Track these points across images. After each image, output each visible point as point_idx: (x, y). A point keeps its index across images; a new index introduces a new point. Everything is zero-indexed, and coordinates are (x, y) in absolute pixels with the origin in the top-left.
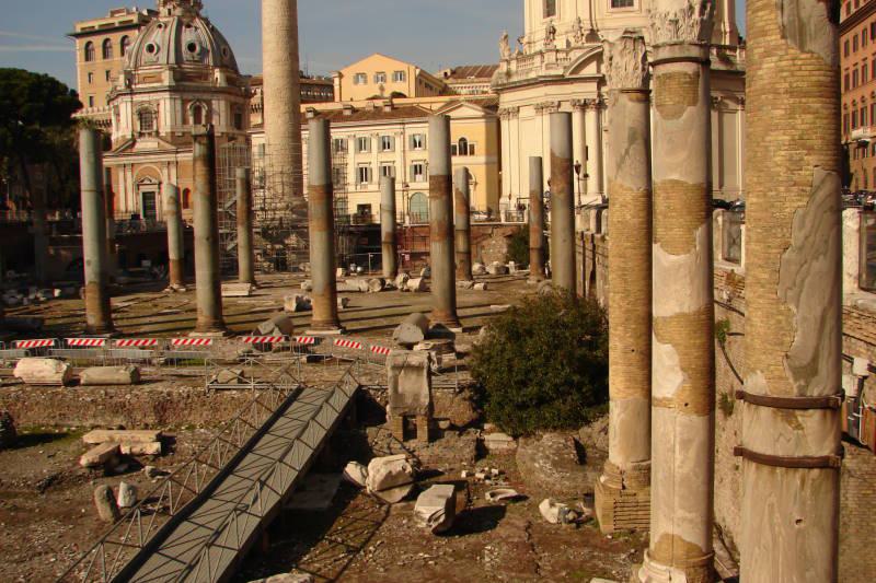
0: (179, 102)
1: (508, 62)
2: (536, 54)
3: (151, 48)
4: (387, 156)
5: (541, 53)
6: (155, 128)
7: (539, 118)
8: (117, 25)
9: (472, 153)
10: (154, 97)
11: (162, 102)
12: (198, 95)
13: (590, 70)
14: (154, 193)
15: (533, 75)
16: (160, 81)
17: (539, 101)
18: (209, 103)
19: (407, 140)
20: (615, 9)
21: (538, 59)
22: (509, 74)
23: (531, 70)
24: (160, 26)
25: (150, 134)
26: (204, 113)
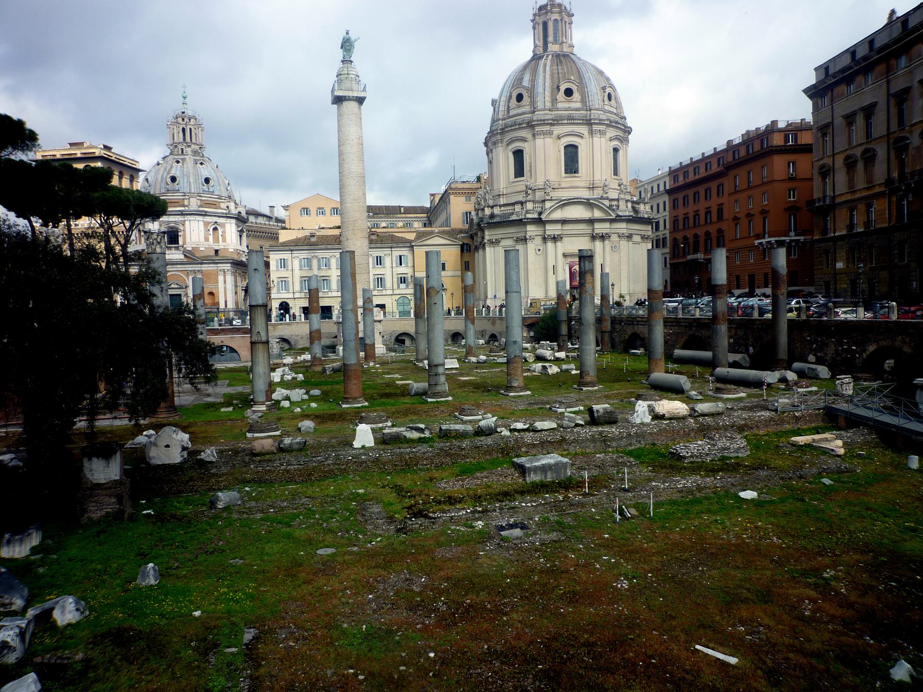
0: (202, 224)
1: (492, 207)
2: (517, 203)
3: (173, 179)
4: (379, 270)
5: (522, 203)
6: (181, 243)
8: (79, 155)
10: (180, 218)
11: (187, 223)
12: (216, 219)
13: (558, 215)
14: (180, 295)
15: (514, 217)
16: (184, 206)
18: (223, 225)
19: (394, 259)
21: (518, 208)
22: (492, 216)
23: (513, 214)
24: (178, 162)
25: (177, 248)
26: (220, 233)
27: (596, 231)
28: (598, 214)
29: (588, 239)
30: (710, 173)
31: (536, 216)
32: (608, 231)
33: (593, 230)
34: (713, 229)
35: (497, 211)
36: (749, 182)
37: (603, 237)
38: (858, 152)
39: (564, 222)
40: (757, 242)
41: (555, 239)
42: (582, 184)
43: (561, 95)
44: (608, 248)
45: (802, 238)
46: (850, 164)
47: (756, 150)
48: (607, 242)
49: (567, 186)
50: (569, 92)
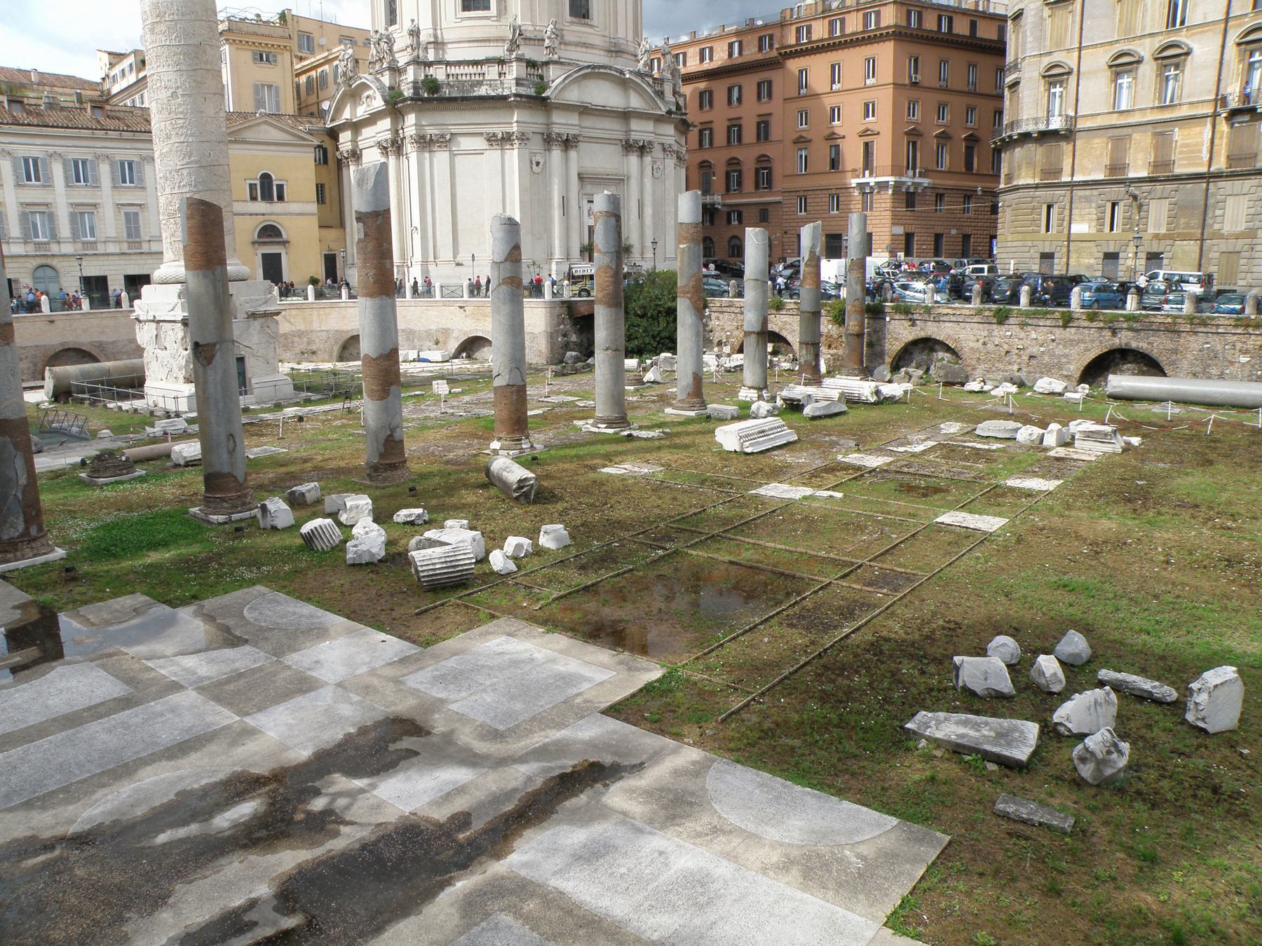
2: (488, 61)
5: (501, 62)
7: (495, 155)
9: (281, 198)
13: (573, 96)
15: (483, 91)
17: (499, 131)
20: (574, 20)
21: (492, 72)
23: (480, 83)
27: (634, 136)
28: (636, 102)
29: (619, 148)
30: (707, 65)
31: (531, 92)
32: (651, 137)
33: (628, 131)
34: (748, 156)
35: (439, 74)
36: (800, 87)
37: (643, 149)
38: (1146, 49)
39: (584, 110)
41: (568, 143)
42: (598, 41)
44: (648, 171)
46: (1122, 65)
47: (849, 30)
48: (648, 159)
49: (576, 39)
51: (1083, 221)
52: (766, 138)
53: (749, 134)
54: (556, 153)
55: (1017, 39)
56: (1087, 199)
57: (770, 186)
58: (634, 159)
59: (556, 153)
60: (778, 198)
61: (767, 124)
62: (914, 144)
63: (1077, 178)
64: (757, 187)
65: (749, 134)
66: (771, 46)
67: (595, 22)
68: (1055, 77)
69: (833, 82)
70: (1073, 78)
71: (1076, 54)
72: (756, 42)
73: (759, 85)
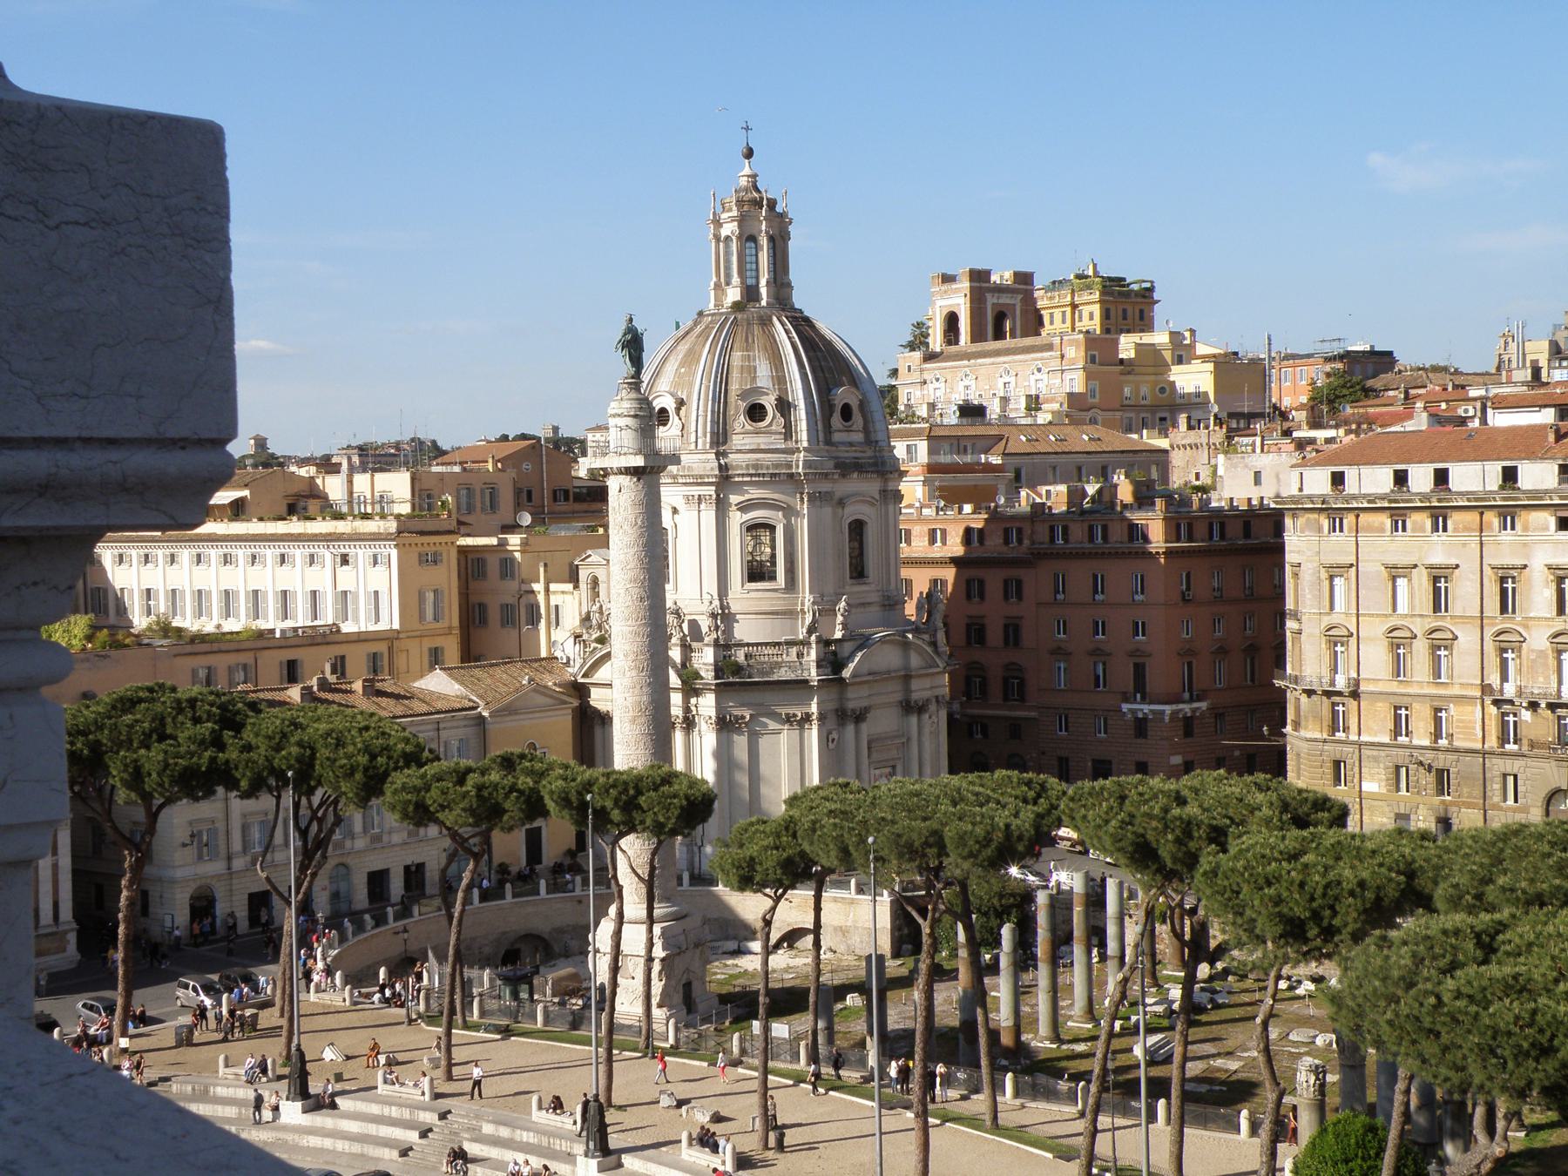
15: (783, 674)
23: (779, 665)
40: (1125, 707)
43: (836, 420)
45: (1203, 705)
50: (846, 412)
51: (1372, 780)
52: (1017, 643)
53: (995, 635)
54: (850, 728)
55: (1296, 585)
56: (1376, 759)
57: (1022, 699)
58: (914, 719)
59: (850, 728)
60: (1033, 714)
61: (1017, 629)
62: (1190, 664)
63: (1364, 738)
64: (1006, 699)
65: (995, 635)
66: (1020, 541)
67: (870, 579)
68: (1335, 640)
69: (1096, 592)
70: (1353, 641)
71: (1354, 620)
72: (1001, 533)
73: (1006, 582)
